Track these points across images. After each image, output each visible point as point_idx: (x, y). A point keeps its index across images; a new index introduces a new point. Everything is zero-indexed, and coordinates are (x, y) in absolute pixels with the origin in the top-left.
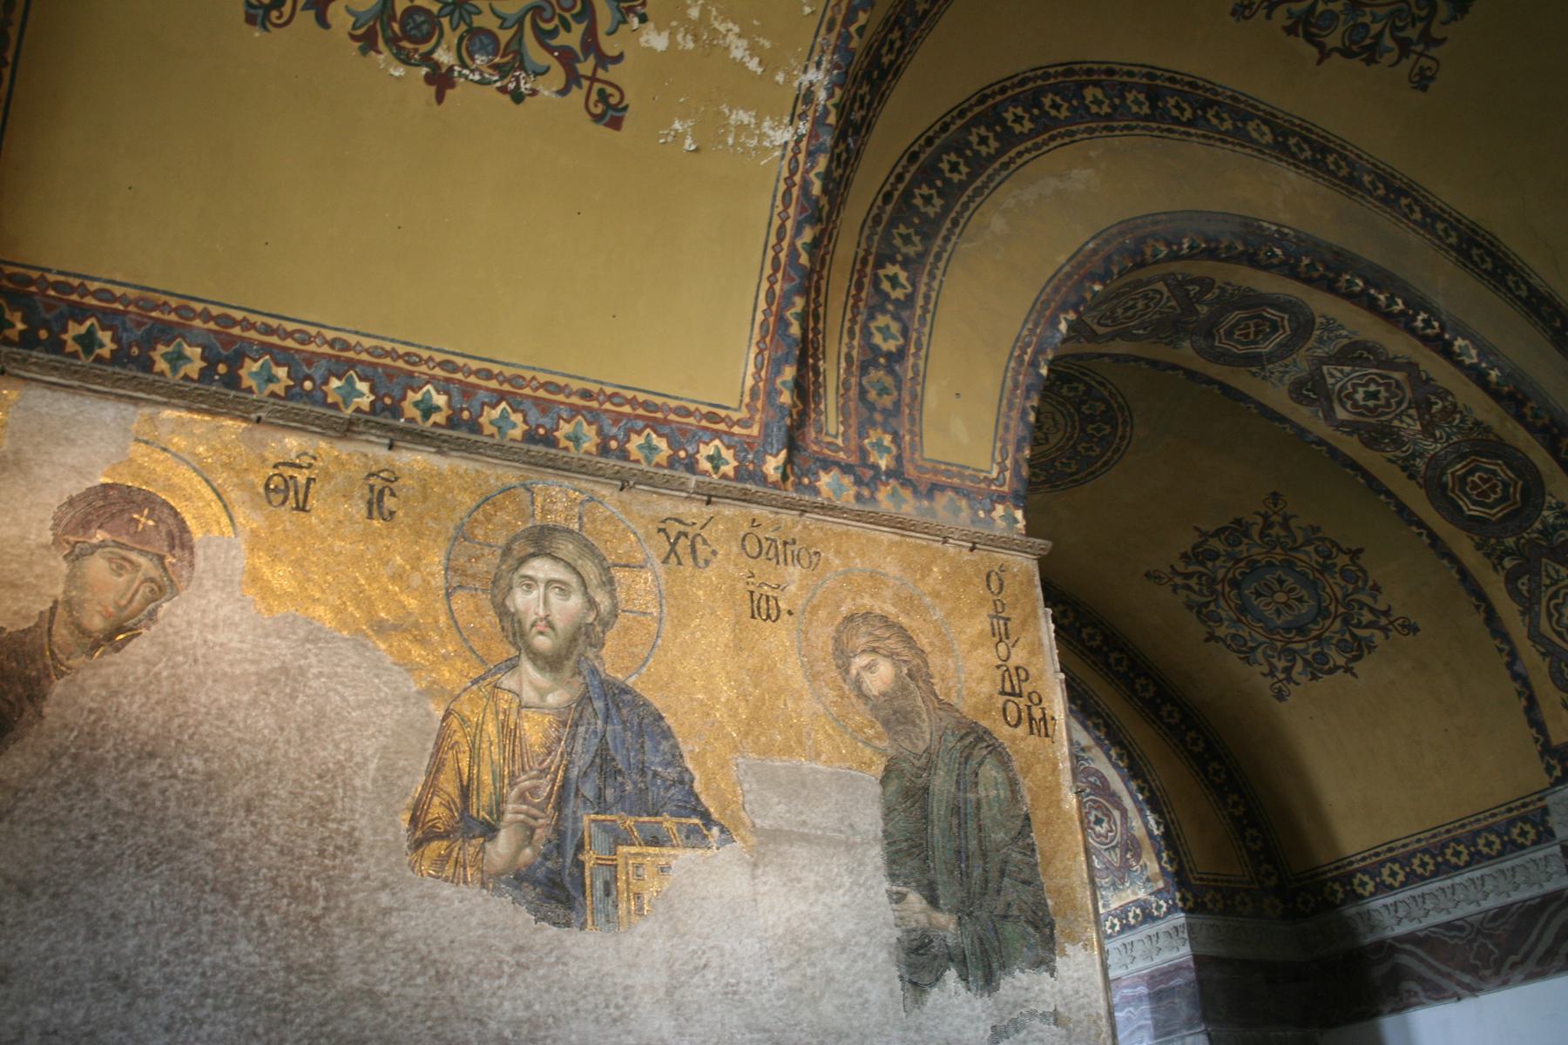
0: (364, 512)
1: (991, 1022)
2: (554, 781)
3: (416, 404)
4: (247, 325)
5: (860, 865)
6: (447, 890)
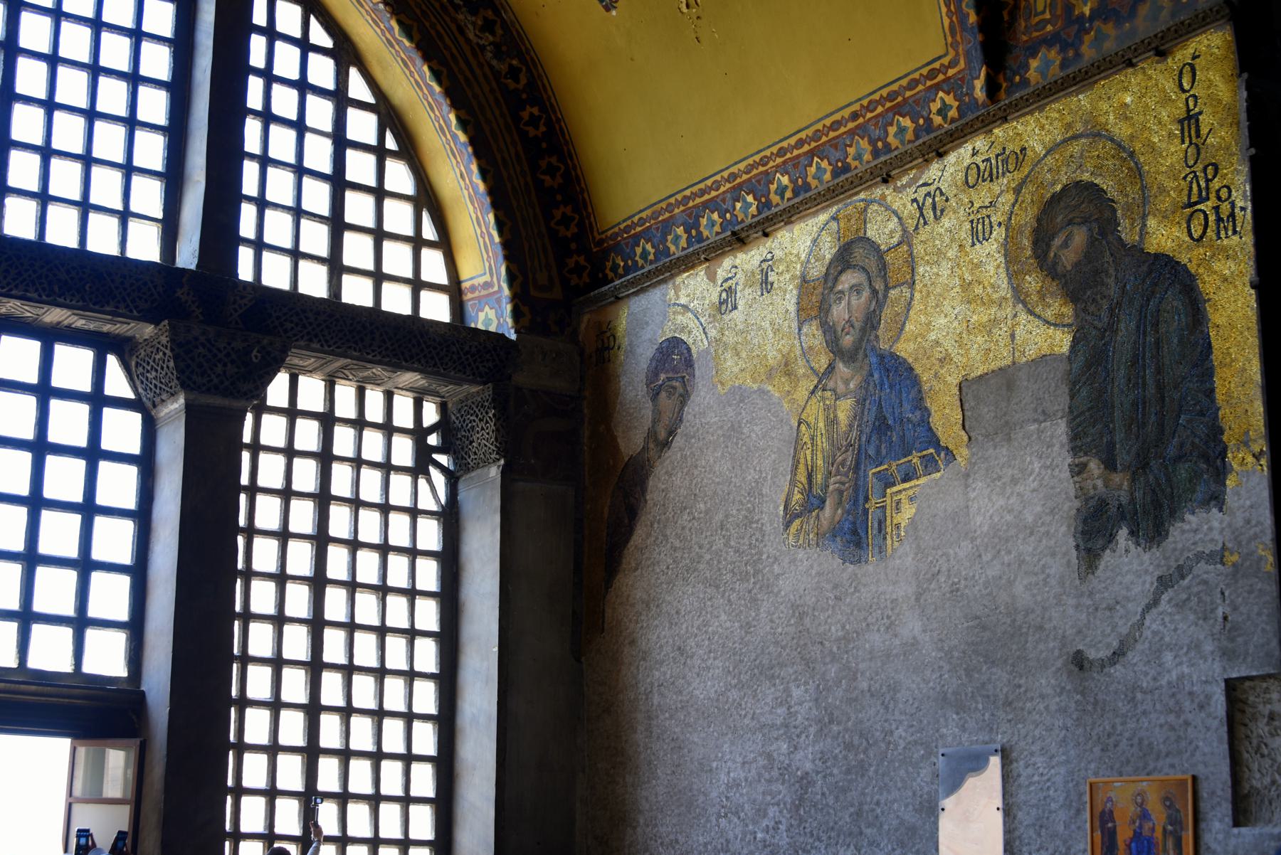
0: (759, 293)
1: (1158, 573)
2: (853, 450)
3: (776, 193)
4: (695, 195)
5: (1048, 447)
6: (801, 554)
